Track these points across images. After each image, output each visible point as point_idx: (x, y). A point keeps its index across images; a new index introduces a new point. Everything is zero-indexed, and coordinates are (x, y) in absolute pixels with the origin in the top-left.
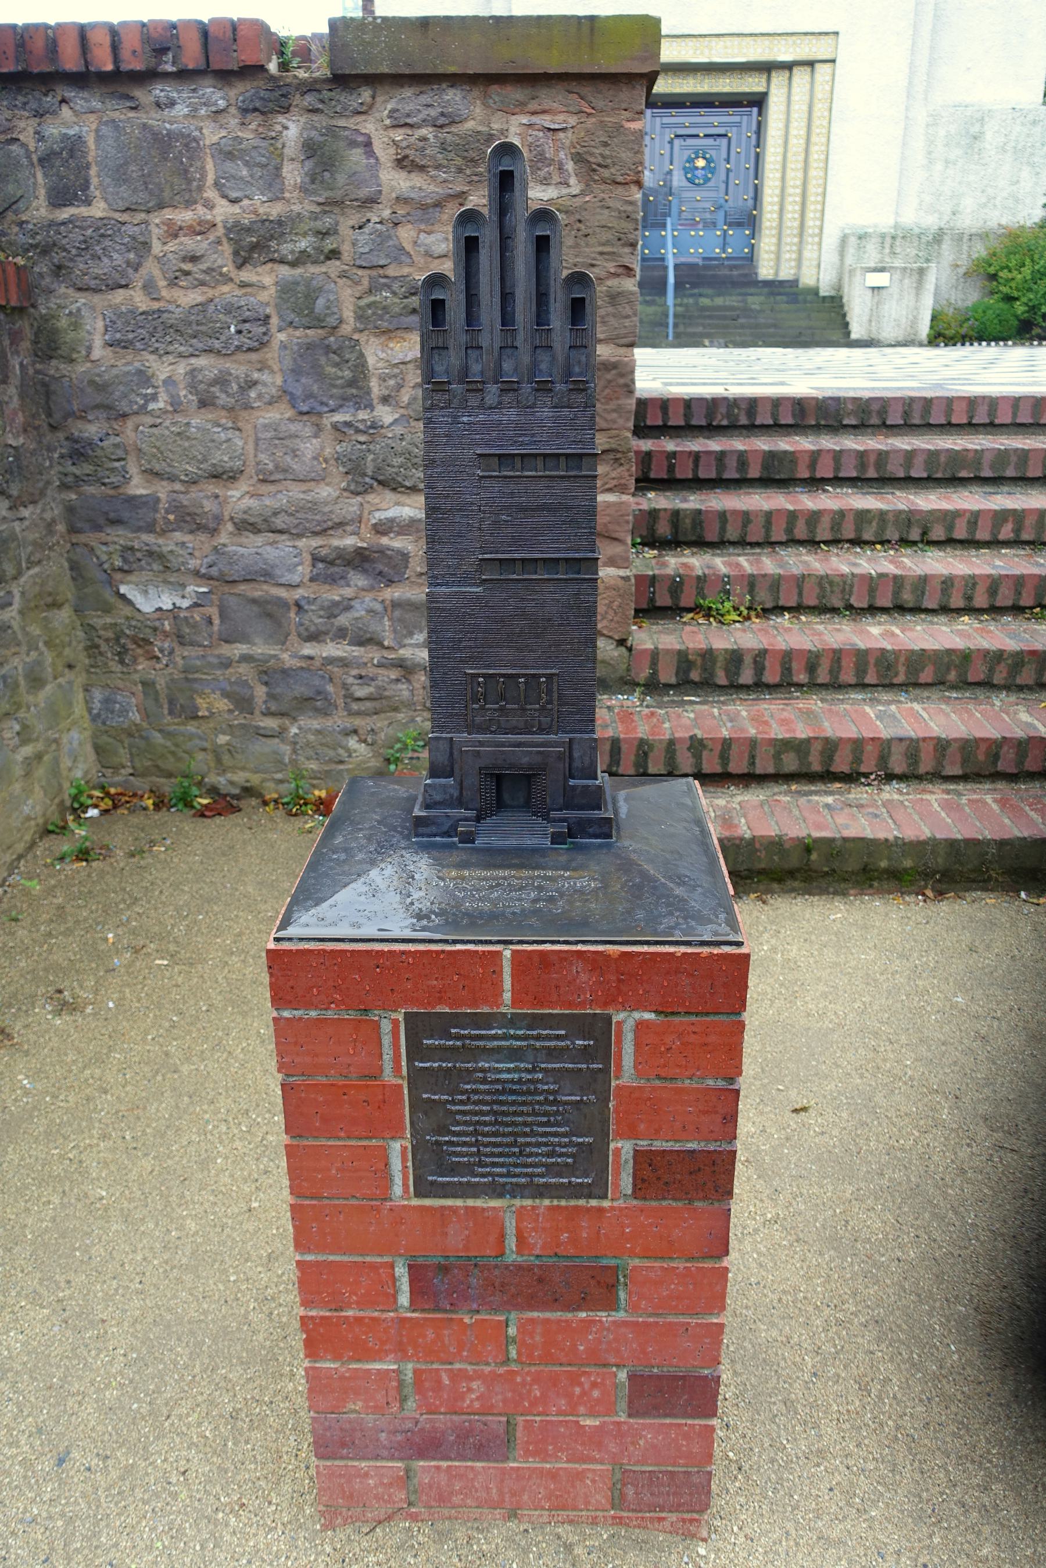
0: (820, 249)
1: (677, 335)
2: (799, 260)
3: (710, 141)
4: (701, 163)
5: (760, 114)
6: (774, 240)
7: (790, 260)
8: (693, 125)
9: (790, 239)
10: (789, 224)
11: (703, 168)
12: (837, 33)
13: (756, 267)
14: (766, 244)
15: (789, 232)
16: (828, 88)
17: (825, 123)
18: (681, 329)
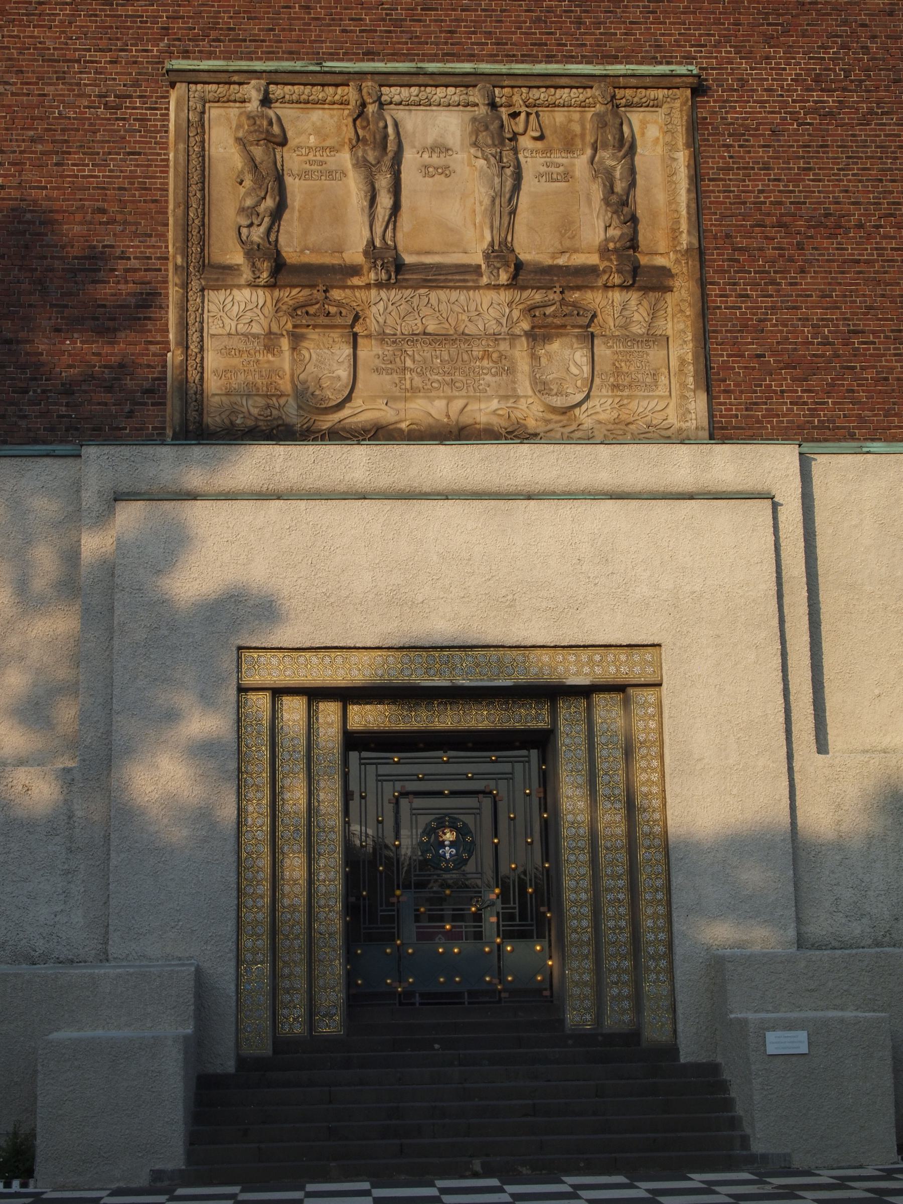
2: (637, 998)
4: (449, 836)
5: (543, 759)
6: (588, 964)
10: (612, 937)
12: (659, 645)
15: (612, 950)
17: (655, 777)
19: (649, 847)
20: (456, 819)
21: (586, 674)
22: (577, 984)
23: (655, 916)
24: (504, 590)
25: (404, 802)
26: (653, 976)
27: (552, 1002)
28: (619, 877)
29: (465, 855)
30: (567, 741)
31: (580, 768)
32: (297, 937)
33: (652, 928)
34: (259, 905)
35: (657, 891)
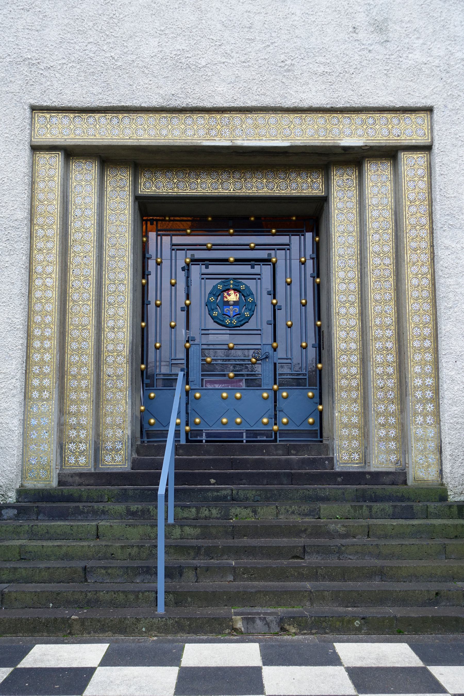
0: (438, 421)
1: (176, 598)
2: (403, 439)
3: (246, 269)
4: (233, 297)
6: (356, 407)
7: (387, 439)
8: (215, 247)
9: (383, 407)
11: (236, 303)
12: (429, 110)
13: (328, 448)
14: (343, 413)
15: (380, 395)
16: (423, 185)
18: (188, 583)
19: (417, 299)
20: (240, 282)
21: (360, 136)
22: (346, 426)
23: (423, 362)
24: (283, 56)
25: (195, 270)
26: (420, 419)
27: (321, 441)
28: (388, 327)
29: (247, 314)
30: (340, 205)
31: (351, 229)
32: (84, 377)
33: (420, 374)
34: (46, 346)
35: (425, 339)
